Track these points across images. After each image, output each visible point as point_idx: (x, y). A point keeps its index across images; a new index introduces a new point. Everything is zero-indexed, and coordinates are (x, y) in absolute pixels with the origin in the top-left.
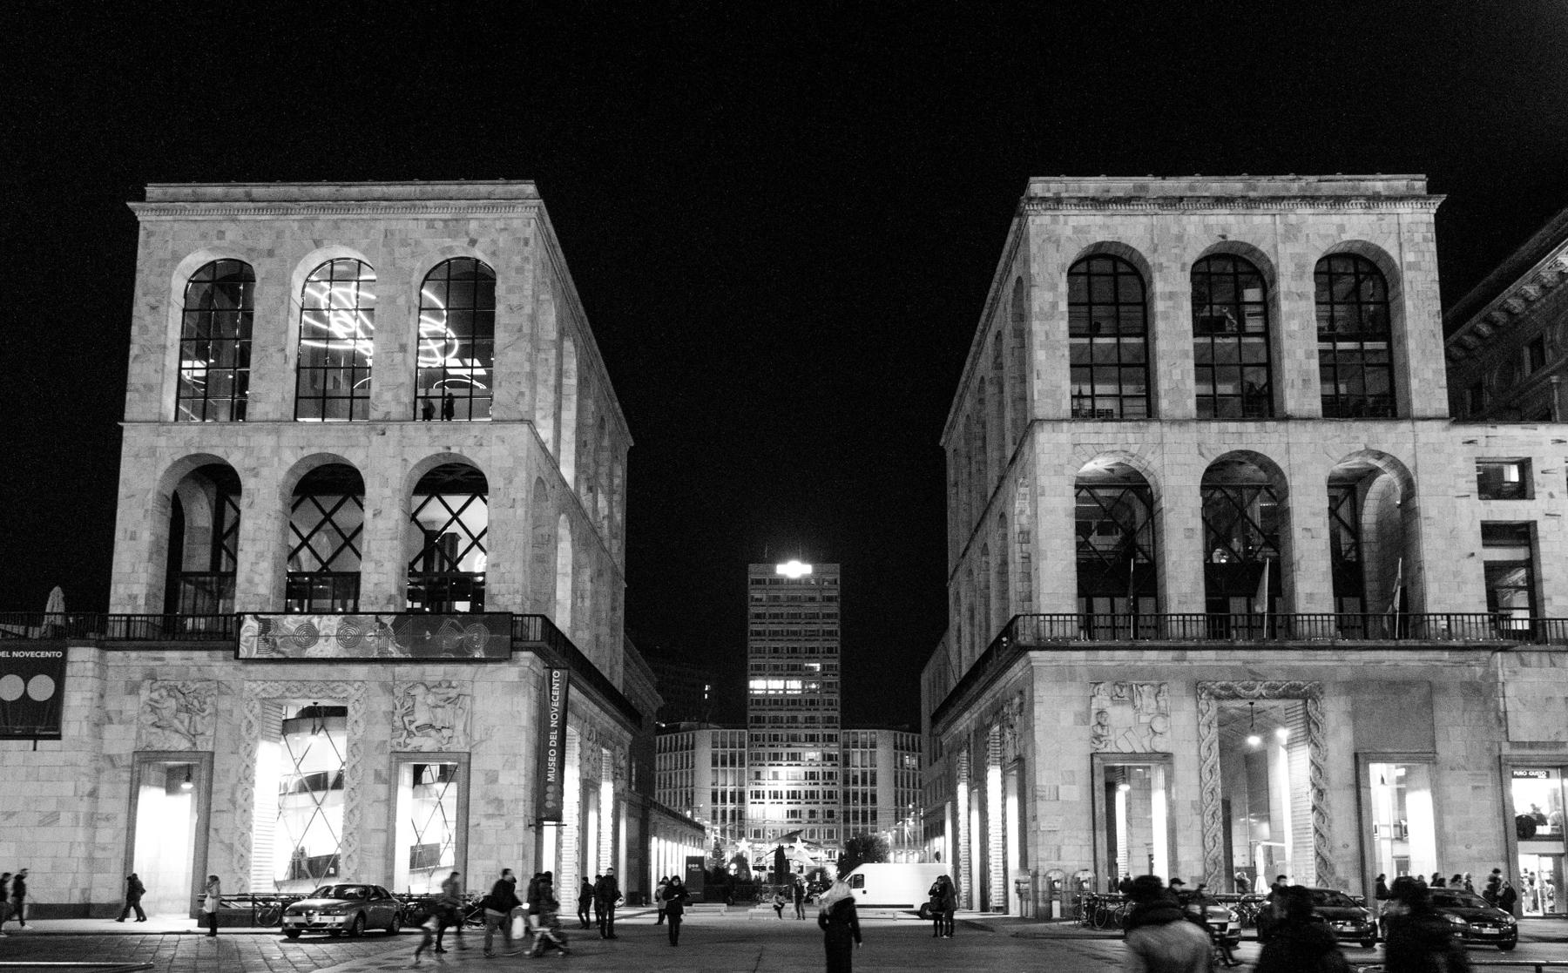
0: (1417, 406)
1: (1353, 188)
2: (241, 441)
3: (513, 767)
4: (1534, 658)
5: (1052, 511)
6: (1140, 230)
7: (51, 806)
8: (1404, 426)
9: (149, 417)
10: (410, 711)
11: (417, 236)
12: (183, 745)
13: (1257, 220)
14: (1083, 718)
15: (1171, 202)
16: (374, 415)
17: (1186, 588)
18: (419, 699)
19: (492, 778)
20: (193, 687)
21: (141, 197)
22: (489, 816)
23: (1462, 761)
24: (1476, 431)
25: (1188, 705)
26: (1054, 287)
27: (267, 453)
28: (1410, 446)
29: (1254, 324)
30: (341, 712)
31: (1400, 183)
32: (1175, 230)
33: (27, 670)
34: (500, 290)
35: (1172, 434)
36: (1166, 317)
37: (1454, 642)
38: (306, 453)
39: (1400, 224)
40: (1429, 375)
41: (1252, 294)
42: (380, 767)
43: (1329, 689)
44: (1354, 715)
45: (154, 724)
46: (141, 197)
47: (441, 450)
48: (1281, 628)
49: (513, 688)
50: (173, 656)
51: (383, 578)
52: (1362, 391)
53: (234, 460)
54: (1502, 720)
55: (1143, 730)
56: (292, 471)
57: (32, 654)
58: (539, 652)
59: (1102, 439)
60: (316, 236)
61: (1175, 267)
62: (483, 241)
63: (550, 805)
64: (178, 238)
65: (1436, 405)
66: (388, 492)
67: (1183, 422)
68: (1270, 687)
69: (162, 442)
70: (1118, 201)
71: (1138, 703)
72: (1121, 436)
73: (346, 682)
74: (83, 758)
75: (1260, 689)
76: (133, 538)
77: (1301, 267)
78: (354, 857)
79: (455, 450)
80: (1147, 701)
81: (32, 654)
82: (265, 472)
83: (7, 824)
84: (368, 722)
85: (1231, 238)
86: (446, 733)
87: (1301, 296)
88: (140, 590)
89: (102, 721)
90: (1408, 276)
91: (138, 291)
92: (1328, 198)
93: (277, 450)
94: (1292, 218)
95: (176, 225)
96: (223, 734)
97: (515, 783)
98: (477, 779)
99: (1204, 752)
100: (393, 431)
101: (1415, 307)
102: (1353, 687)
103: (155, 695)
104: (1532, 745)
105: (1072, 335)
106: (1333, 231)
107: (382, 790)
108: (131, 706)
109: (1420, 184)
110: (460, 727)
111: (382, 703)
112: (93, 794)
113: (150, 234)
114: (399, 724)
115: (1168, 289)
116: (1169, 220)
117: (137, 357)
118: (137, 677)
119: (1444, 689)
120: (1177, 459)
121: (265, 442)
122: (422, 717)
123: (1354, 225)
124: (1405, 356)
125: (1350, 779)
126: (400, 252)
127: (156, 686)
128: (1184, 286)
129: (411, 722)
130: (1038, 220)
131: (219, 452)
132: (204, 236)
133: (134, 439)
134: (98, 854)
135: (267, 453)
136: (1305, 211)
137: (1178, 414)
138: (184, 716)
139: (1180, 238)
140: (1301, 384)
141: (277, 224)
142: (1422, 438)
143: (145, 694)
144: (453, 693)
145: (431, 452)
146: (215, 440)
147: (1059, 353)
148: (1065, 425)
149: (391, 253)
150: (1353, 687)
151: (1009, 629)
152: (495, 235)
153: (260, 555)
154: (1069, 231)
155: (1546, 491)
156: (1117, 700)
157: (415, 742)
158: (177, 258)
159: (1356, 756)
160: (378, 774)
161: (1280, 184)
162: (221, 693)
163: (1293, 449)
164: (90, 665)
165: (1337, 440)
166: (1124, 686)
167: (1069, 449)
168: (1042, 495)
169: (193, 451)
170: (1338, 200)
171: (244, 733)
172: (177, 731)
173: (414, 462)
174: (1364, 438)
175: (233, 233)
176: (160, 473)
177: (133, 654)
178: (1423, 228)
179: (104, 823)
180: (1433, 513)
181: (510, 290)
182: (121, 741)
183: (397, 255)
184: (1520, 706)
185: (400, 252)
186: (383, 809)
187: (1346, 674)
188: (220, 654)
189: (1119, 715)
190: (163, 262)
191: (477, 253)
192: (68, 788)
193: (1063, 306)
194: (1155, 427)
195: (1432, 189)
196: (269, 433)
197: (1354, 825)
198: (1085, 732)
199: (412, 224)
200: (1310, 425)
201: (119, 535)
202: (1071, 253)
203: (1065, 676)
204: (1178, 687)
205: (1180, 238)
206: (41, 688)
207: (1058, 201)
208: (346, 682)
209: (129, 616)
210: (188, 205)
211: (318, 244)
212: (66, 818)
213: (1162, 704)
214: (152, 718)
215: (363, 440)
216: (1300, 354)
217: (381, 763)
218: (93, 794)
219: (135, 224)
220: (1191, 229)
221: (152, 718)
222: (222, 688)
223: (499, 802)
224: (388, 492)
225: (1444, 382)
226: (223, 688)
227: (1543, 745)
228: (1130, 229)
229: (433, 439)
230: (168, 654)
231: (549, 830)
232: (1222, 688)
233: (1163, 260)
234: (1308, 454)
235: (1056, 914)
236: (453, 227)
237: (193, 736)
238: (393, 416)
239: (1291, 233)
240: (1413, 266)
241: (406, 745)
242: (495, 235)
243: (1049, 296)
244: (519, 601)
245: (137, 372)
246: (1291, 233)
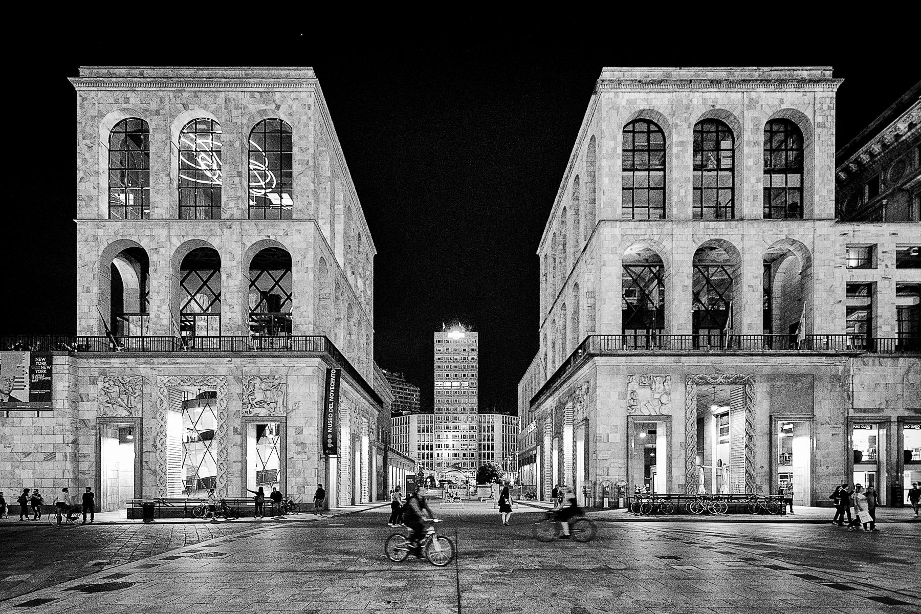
0: (817, 212)
1: (790, 75)
2: (147, 232)
3: (311, 425)
4: (870, 361)
5: (610, 275)
6: (665, 102)
7: (50, 449)
8: (809, 224)
9: (92, 217)
10: (252, 393)
11: (244, 102)
12: (125, 413)
13: (733, 95)
14: (623, 396)
16: (224, 216)
17: (682, 321)
18: (257, 386)
19: (299, 431)
21: (77, 74)
23: (828, 420)
24: (847, 228)
25: (681, 388)
26: (614, 138)
27: (163, 239)
28: (811, 236)
29: (726, 163)
30: (213, 395)
31: (816, 72)
32: (685, 102)
34: (295, 138)
35: (677, 229)
36: (678, 157)
37: (830, 352)
38: (186, 239)
39: (813, 98)
40: (825, 193)
41: (726, 144)
43: (758, 378)
44: (771, 394)
46: (77, 74)
47: (265, 238)
48: (733, 345)
49: (308, 379)
50: (115, 361)
51: (234, 315)
52: (786, 207)
53: (145, 244)
54: (850, 397)
55: (656, 403)
56: (178, 250)
58: (323, 357)
59: (639, 232)
60: (184, 102)
61: (685, 125)
62: (284, 107)
63: (330, 445)
64: (102, 102)
65: (827, 211)
66: (234, 263)
67: (685, 221)
68: (726, 378)
69: (101, 232)
70: (653, 82)
71: (653, 387)
72: (649, 230)
73: (215, 376)
74: (67, 421)
75: (720, 379)
76: (88, 291)
77: (757, 125)
79: (272, 238)
80: (659, 386)
82: (162, 250)
83: (26, 459)
84: (228, 400)
85: (717, 107)
87: (756, 144)
89: (76, 400)
90: (818, 131)
91: (79, 136)
92: (776, 81)
93: (169, 237)
94: (754, 95)
95: (100, 94)
96: (147, 406)
97: (312, 434)
98: (291, 432)
99: (689, 415)
100: (236, 226)
101: (820, 151)
102: (771, 378)
103: (106, 385)
104: (865, 411)
105: (624, 170)
106: (776, 102)
107: (238, 439)
108: (93, 391)
109: (828, 72)
111: (236, 389)
112: (75, 442)
113: (84, 99)
115: (681, 139)
117: (82, 178)
118: (96, 374)
119: (821, 379)
120: (679, 244)
121: (162, 232)
122: (259, 396)
124: (813, 181)
125: (767, 429)
126: (235, 113)
127: (107, 379)
128: (690, 138)
129: (253, 400)
130: (607, 95)
131: (135, 239)
132: (116, 101)
133: (84, 230)
134: (80, 476)
135: (163, 239)
137: (682, 216)
138: (124, 397)
139: (688, 107)
140: (751, 200)
141: (160, 94)
142: (818, 232)
143: (100, 384)
144: (276, 382)
145: (259, 239)
146: (132, 231)
147: (616, 180)
148: (618, 223)
149: (230, 113)
150: (771, 378)
151: (583, 346)
152: (290, 102)
153: (163, 301)
154: (624, 103)
155: (884, 264)
156: (642, 385)
157: (256, 411)
158: (101, 115)
159: (771, 416)
160: (235, 429)
161: (748, 73)
162: (145, 383)
163: (746, 238)
164: (66, 367)
165: (771, 233)
166: (647, 378)
167: (620, 238)
168: (604, 265)
169: (120, 238)
171: (158, 406)
172: (120, 406)
173: (249, 245)
174: (785, 231)
175: (134, 99)
176: (101, 252)
177: (92, 361)
178: (828, 101)
179: (83, 459)
180: (821, 276)
181: (300, 138)
182: (89, 412)
183: (233, 115)
184: (861, 389)
185: (235, 113)
186: (238, 449)
187: (767, 370)
188: (142, 360)
189: (643, 394)
190: (93, 118)
191: (282, 115)
192: (59, 439)
193: (620, 150)
194: (669, 225)
195: (836, 75)
196: (163, 227)
197: (767, 456)
198: (624, 403)
199: (241, 95)
200: (755, 224)
201: (79, 289)
202: (627, 117)
203: (614, 371)
204: (676, 377)
205: (688, 107)
208: (215, 376)
209: (87, 337)
210: (105, 80)
211: (186, 107)
212: (59, 456)
213: (667, 387)
214: (106, 398)
215: (219, 232)
216: (753, 180)
217: (237, 423)
218: (75, 442)
219: (72, 94)
220: (695, 101)
221: (106, 398)
222: (144, 380)
223: (303, 445)
224: (234, 263)
225: (833, 197)
227: (872, 410)
228: (658, 101)
229: (259, 231)
230: (112, 360)
231: (333, 461)
232: (700, 378)
233: (678, 121)
234: (752, 240)
235: (606, 505)
236: (265, 97)
237: (129, 408)
238: (236, 217)
239: (752, 104)
240: (822, 125)
241: (251, 412)
242: (290, 102)
243: (612, 144)
244: (311, 329)
245: (83, 188)
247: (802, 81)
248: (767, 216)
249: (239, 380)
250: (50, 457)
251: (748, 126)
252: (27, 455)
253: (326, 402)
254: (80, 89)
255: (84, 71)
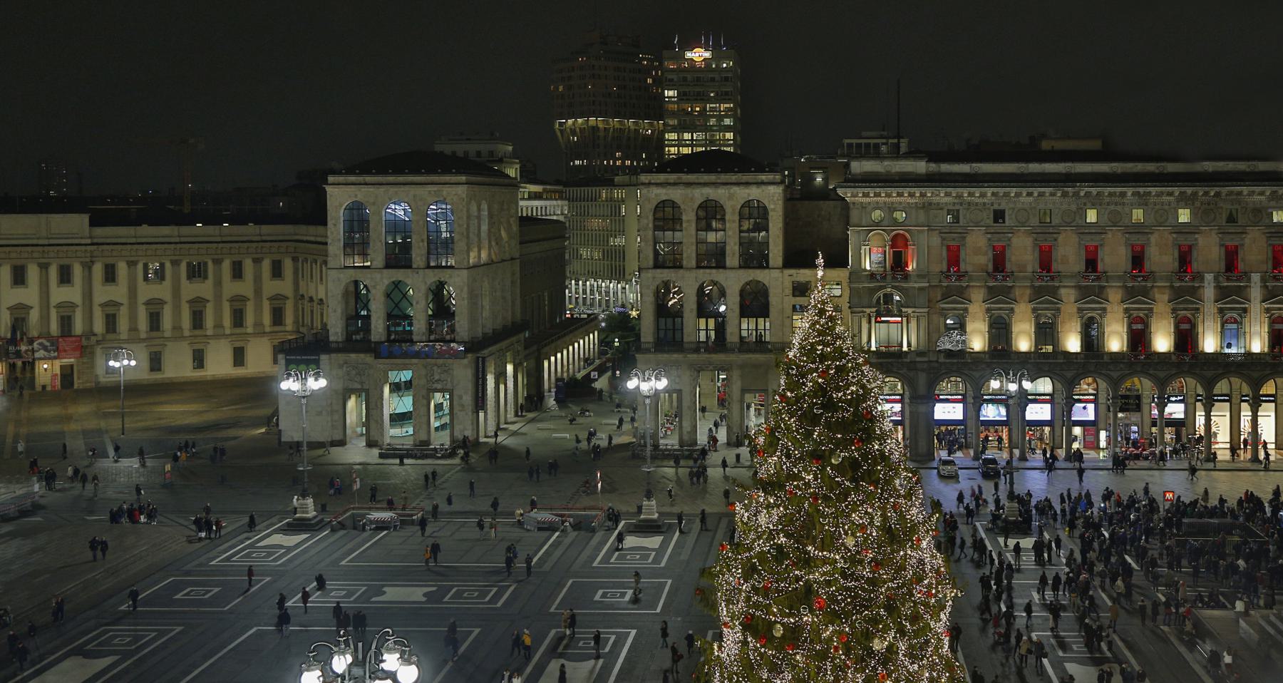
8: (767, 271)
15: (689, 184)
16: (414, 266)
19: (461, 397)
50: (353, 356)
70: (670, 184)
88: (339, 330)
90: (771, 213)
97: (468, 399)
116: (689, 191)
121: (378, 276)
122: (437, 377)
123: (754, 193)
136: (735, 189)
170: (747, 184)
207: (650, 184)
217: (424, 392)
223: (463, 406)
228: (676, 194)
231: (481, 415)
240: (774, 210)
246: (731, 197)
247: (763, 183)
248: (740, 267)
249: (425, 367)
251: (728, 210)
253: (477, 379)
254: (329, 189)
255: (331, 179)
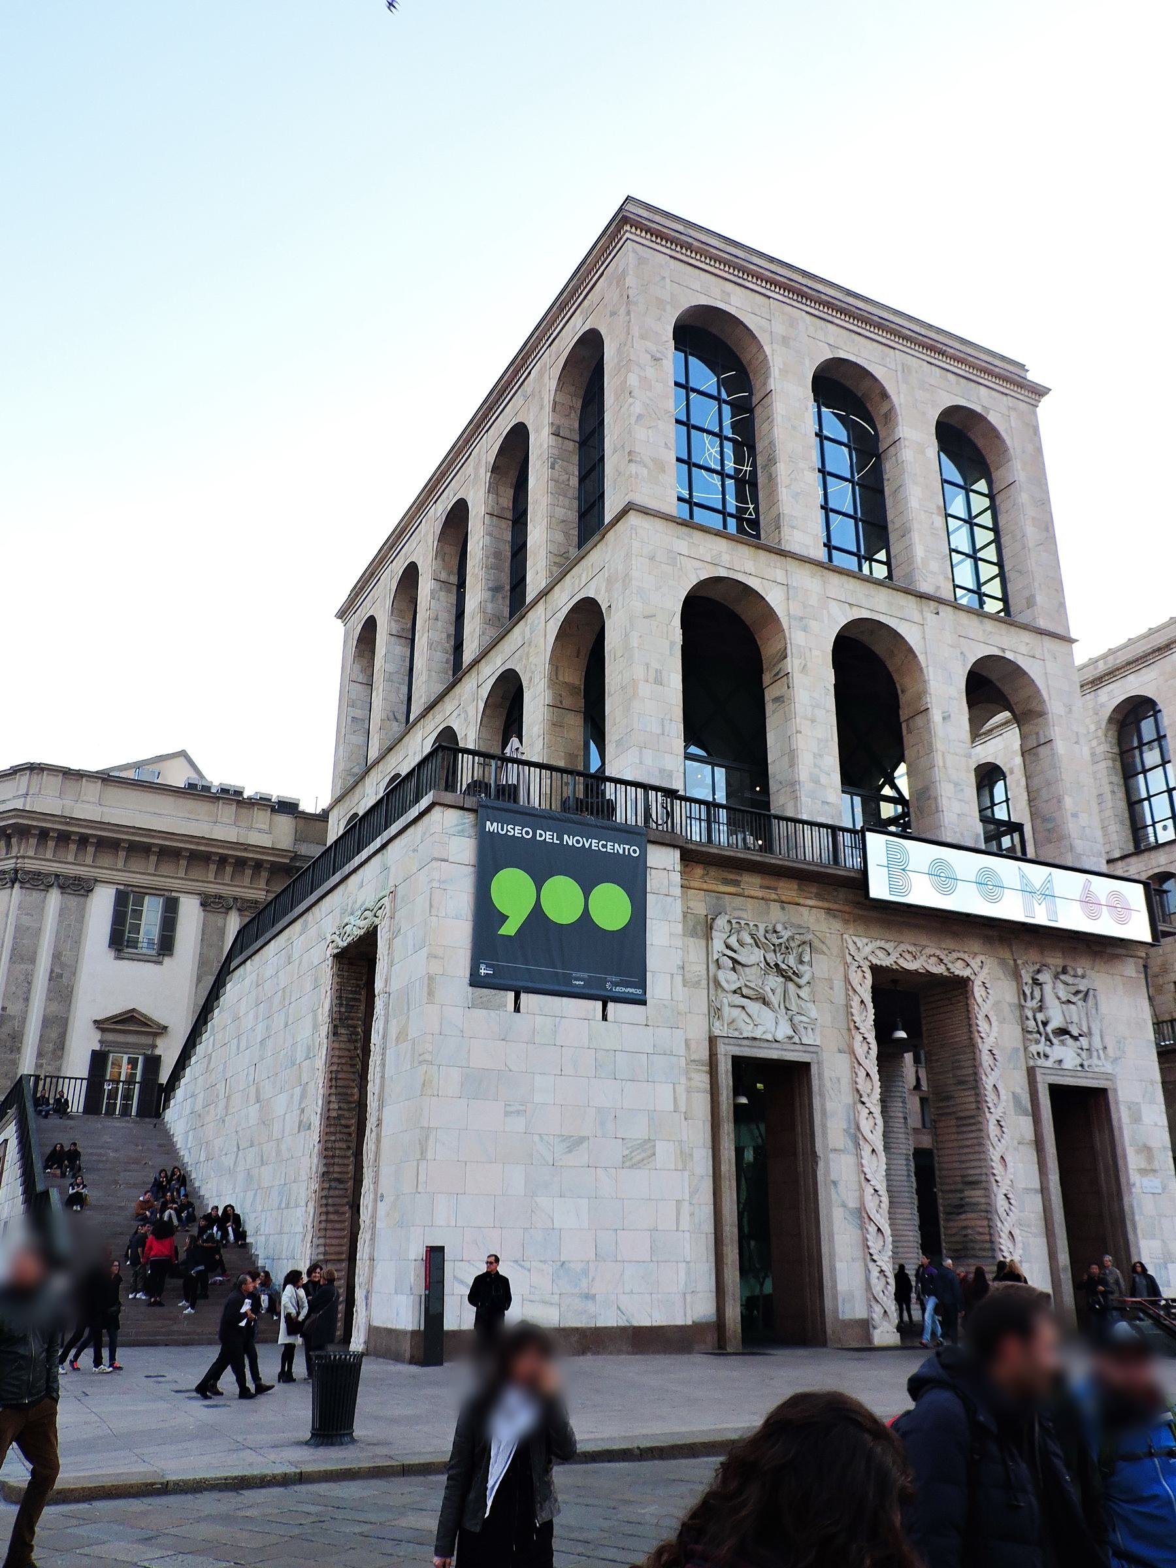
18: (1048, 988)
20: (786, 934)
22: (1143, 1172)
33: (589, 873)
42: (1018, 1090)
45: (735, 992)
57: (594, 844)
78: (1016, 1232)
81: (594, 844)
86: (1084, 1041)
103: (733, 941)
110: (1096, 1040)
114: (1031, 1024)
129: (1045, 1024)
138: (775, 981)
206: (610, 908)
226: (816, 943)
241: (1046, 1056)
250: (640, 1155)
252: (574, 1143)
